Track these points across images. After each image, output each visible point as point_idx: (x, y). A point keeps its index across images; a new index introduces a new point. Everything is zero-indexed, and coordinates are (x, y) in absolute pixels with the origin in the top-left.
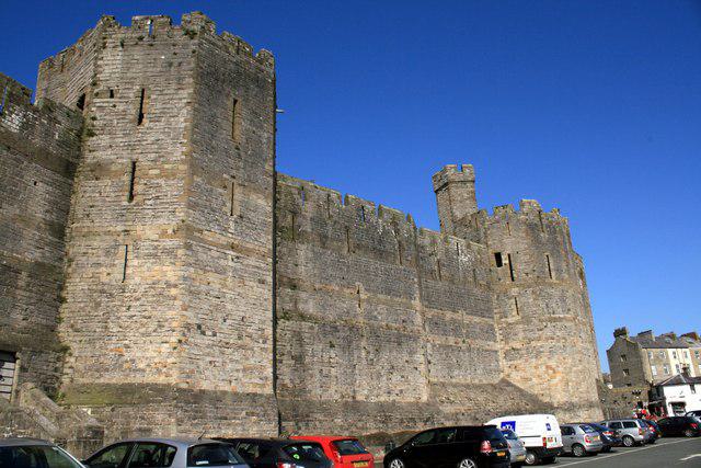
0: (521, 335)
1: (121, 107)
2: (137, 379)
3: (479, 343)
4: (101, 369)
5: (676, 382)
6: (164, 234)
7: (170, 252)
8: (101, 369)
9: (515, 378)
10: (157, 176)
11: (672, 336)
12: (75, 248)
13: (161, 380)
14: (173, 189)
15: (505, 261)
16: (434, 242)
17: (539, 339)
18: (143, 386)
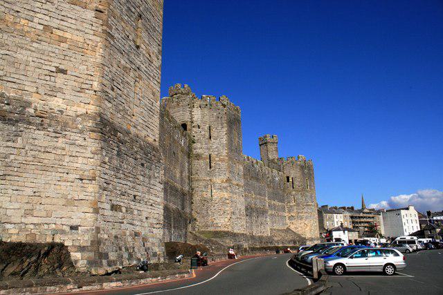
0: (295, 211)
1: (203, 133)
2: (219, 229)
3: (280, 213)
4: (207, 226)
5: (338, 229)
6: (222, 182)
7: (225, 188)
8: (207, 226)
9: (292, 227)
11: (336, 208)
12: (195, 185)
13: (226, 230)
14: (224, 165)
15: (291, 180)
16: (269, 172)
17: (302, 213)
18: (220, 232)
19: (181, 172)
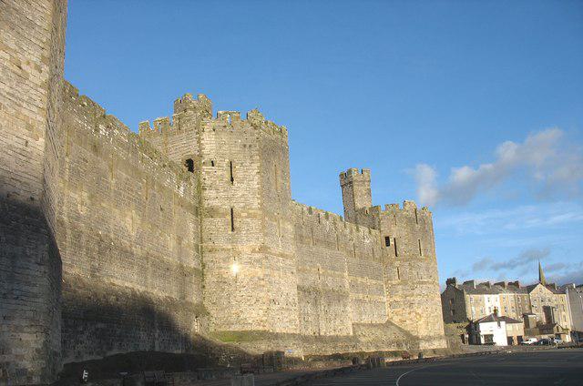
1: (219, 173)
2: (248, 328)
3: (375, 297)
5: (489, 319)
6: (254, 251)
7: (258, 261)
8: (229, 324)
9: (396, 320)
10: (246, 217)
11: (487, 284)
12: (208, 257)
13: (261, 328)
14: (255, 224)
15: (392, 243)
17: (413, 295)
18: (251, 332)
19: (180, 239)
